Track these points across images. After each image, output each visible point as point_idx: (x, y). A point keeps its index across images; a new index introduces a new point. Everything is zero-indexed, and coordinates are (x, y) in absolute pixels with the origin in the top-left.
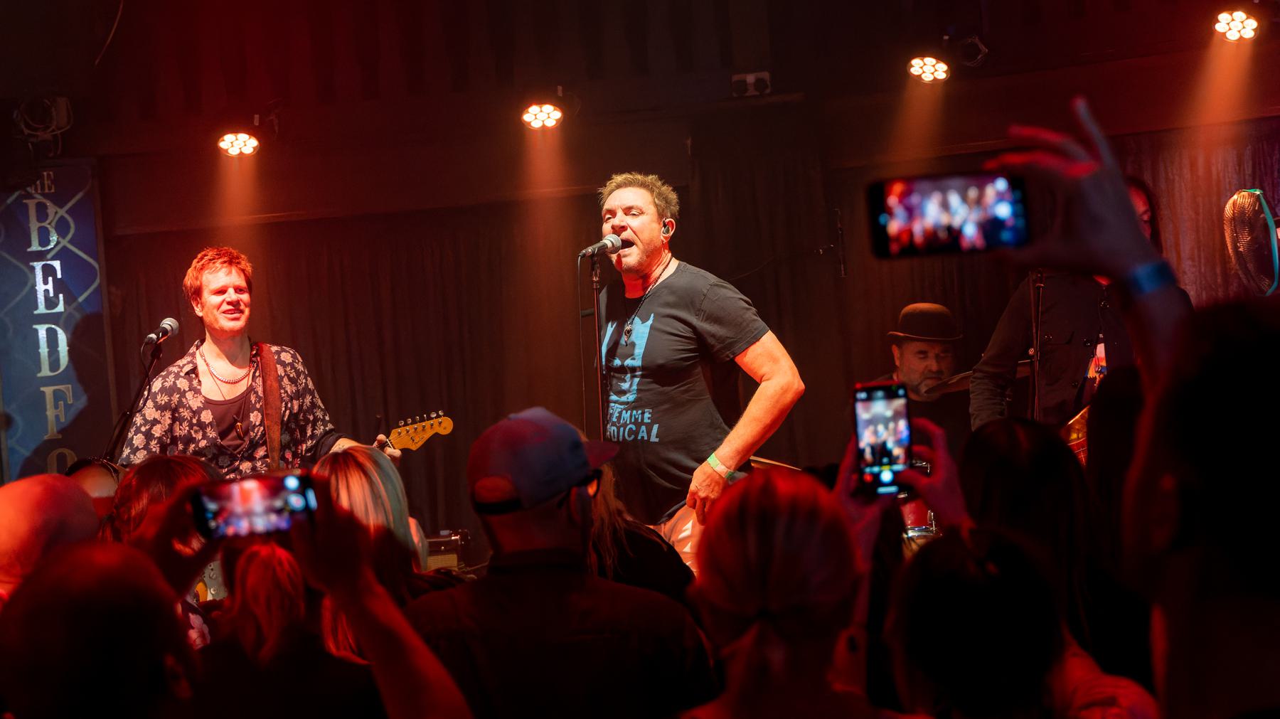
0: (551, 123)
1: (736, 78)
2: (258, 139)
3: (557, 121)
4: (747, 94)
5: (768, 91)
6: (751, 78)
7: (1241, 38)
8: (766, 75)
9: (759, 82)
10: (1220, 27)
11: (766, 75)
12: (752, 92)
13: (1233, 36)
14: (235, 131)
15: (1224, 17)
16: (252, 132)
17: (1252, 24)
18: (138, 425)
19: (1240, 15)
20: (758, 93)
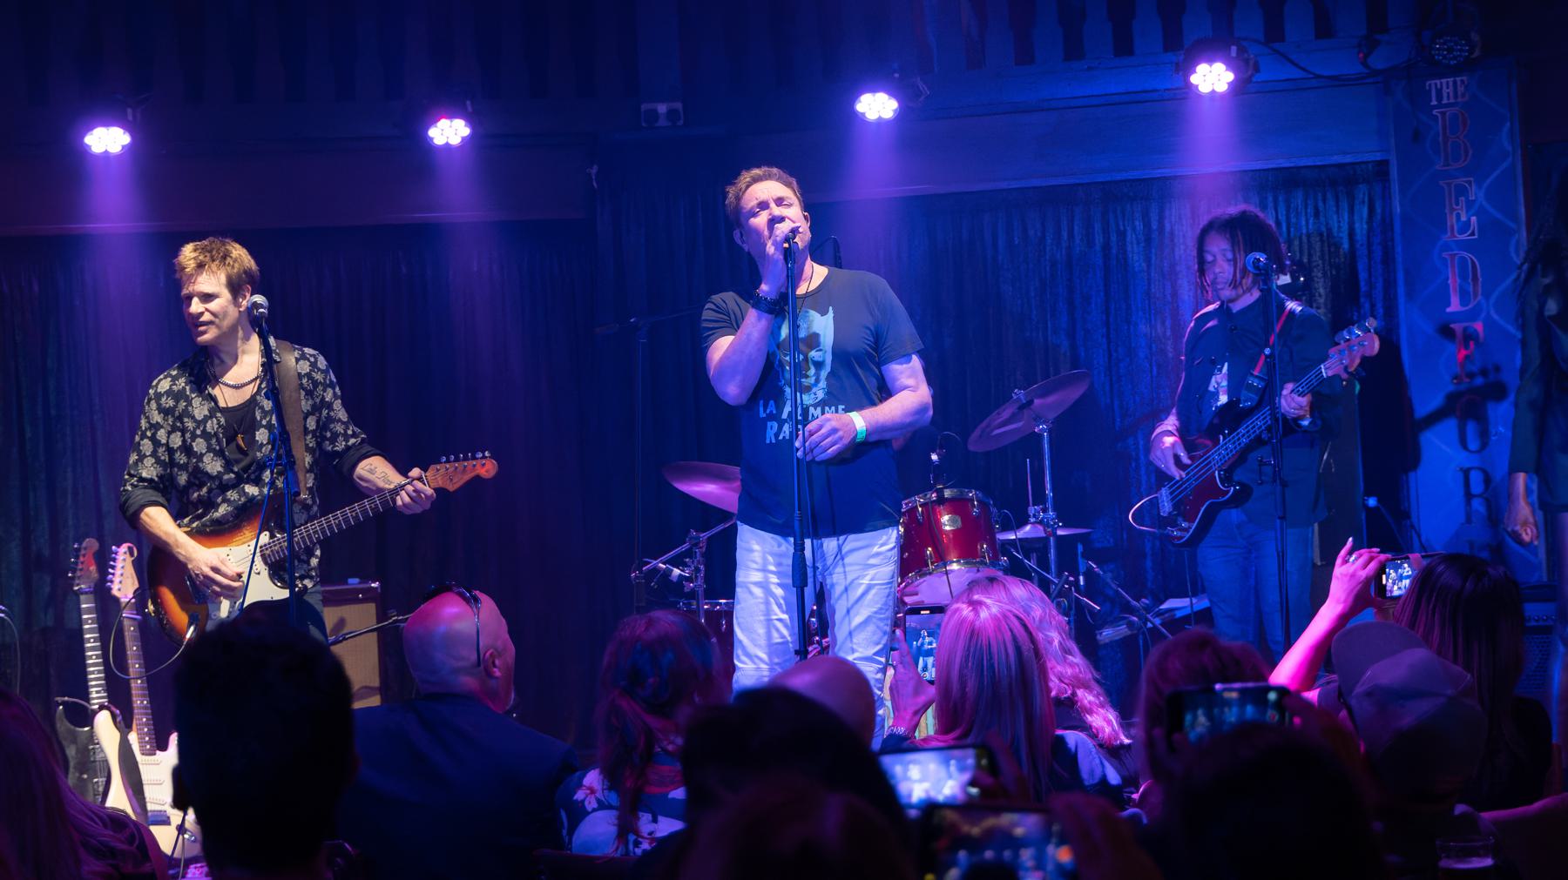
0: (455, 141)
1: (644, 107)
2: (133, 136)
3: (463, 139)
4: (657, 125)
5: (681, 122)
6: (662, 108)
7: (1213, 91)
8: (679, 106)
9: (671, 113)
10: (1194, 79)
11: (679, 106)
12: (662, 122)
13: (1204, 89)
14: (107, 124)
15: (1202, 68)
16: (127, 127)
17: (1230, 76)
18: (143, 428)
19: (1219, 67)
20: (670, 124)
